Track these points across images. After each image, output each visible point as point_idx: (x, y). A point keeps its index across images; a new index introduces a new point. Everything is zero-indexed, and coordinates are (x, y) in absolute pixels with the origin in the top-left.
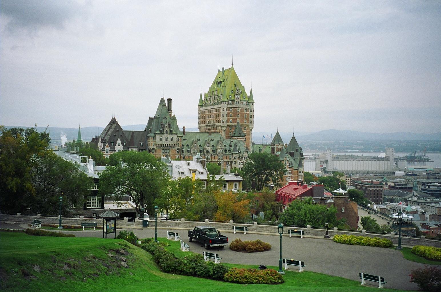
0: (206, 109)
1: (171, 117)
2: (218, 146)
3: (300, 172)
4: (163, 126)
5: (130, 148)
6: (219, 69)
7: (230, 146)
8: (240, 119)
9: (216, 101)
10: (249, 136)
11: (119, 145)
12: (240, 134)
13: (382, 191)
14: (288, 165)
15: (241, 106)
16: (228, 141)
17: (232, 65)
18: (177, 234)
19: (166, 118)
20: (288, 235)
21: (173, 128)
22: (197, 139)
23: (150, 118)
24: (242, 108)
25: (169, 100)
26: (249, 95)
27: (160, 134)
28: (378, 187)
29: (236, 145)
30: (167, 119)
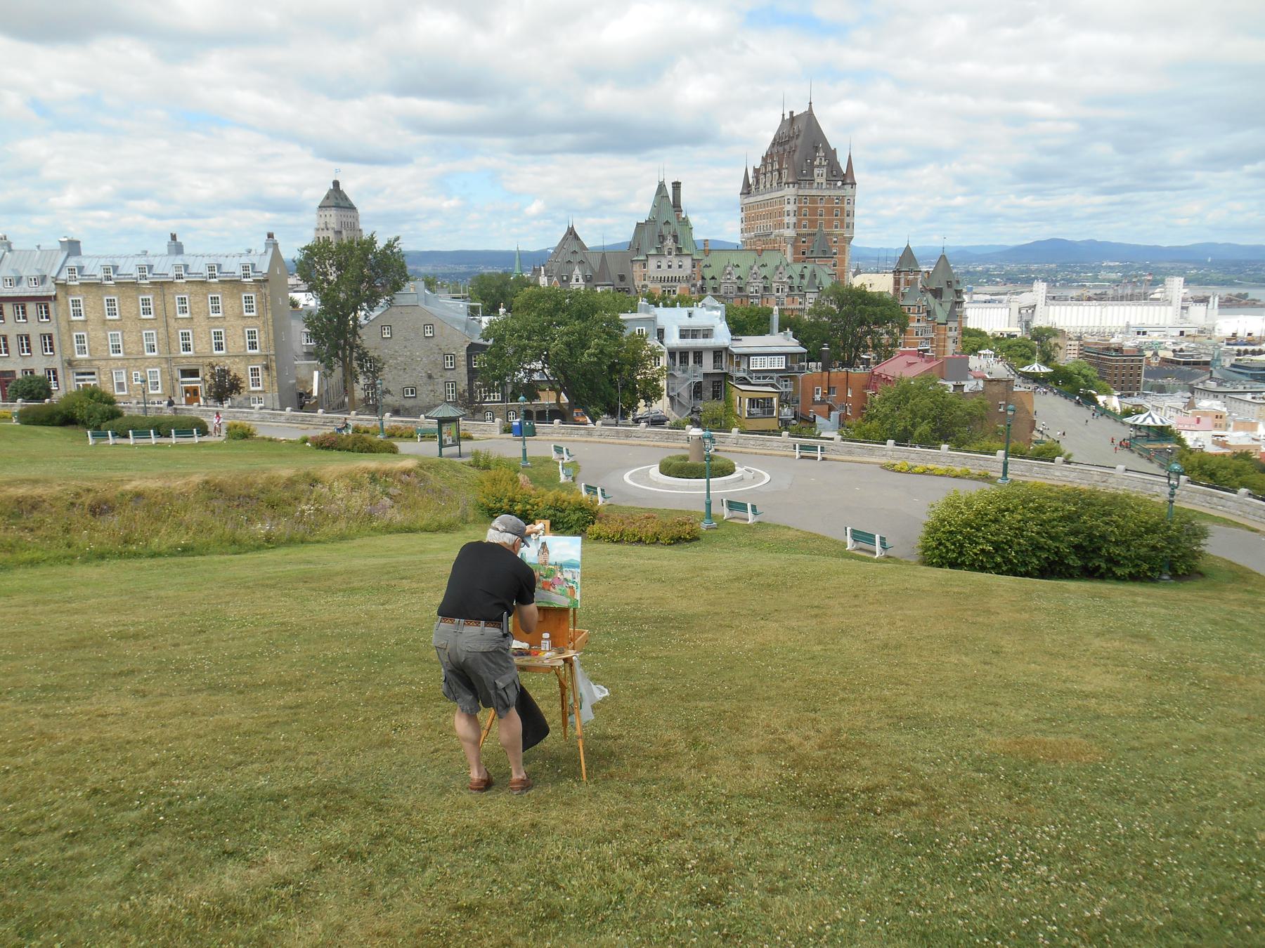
1: (681, 219)
2: (776, 278)
4: (662, 238)
5: (599, 285)
6: (783, 115)
7: (802, 277)
9: (775, 184)
11: (577, 280)
12: (824, 252)
13: (1140, 368)
14: (925, 314)
15: (827, 193)
16: (798, 268)
17: (810, 103)
18: (567, 450)
19: (667, 222)
20: (792, 454)
21: (684, 243)
23: (638, 224)
28: (1132, 361)
29: (814, 276)
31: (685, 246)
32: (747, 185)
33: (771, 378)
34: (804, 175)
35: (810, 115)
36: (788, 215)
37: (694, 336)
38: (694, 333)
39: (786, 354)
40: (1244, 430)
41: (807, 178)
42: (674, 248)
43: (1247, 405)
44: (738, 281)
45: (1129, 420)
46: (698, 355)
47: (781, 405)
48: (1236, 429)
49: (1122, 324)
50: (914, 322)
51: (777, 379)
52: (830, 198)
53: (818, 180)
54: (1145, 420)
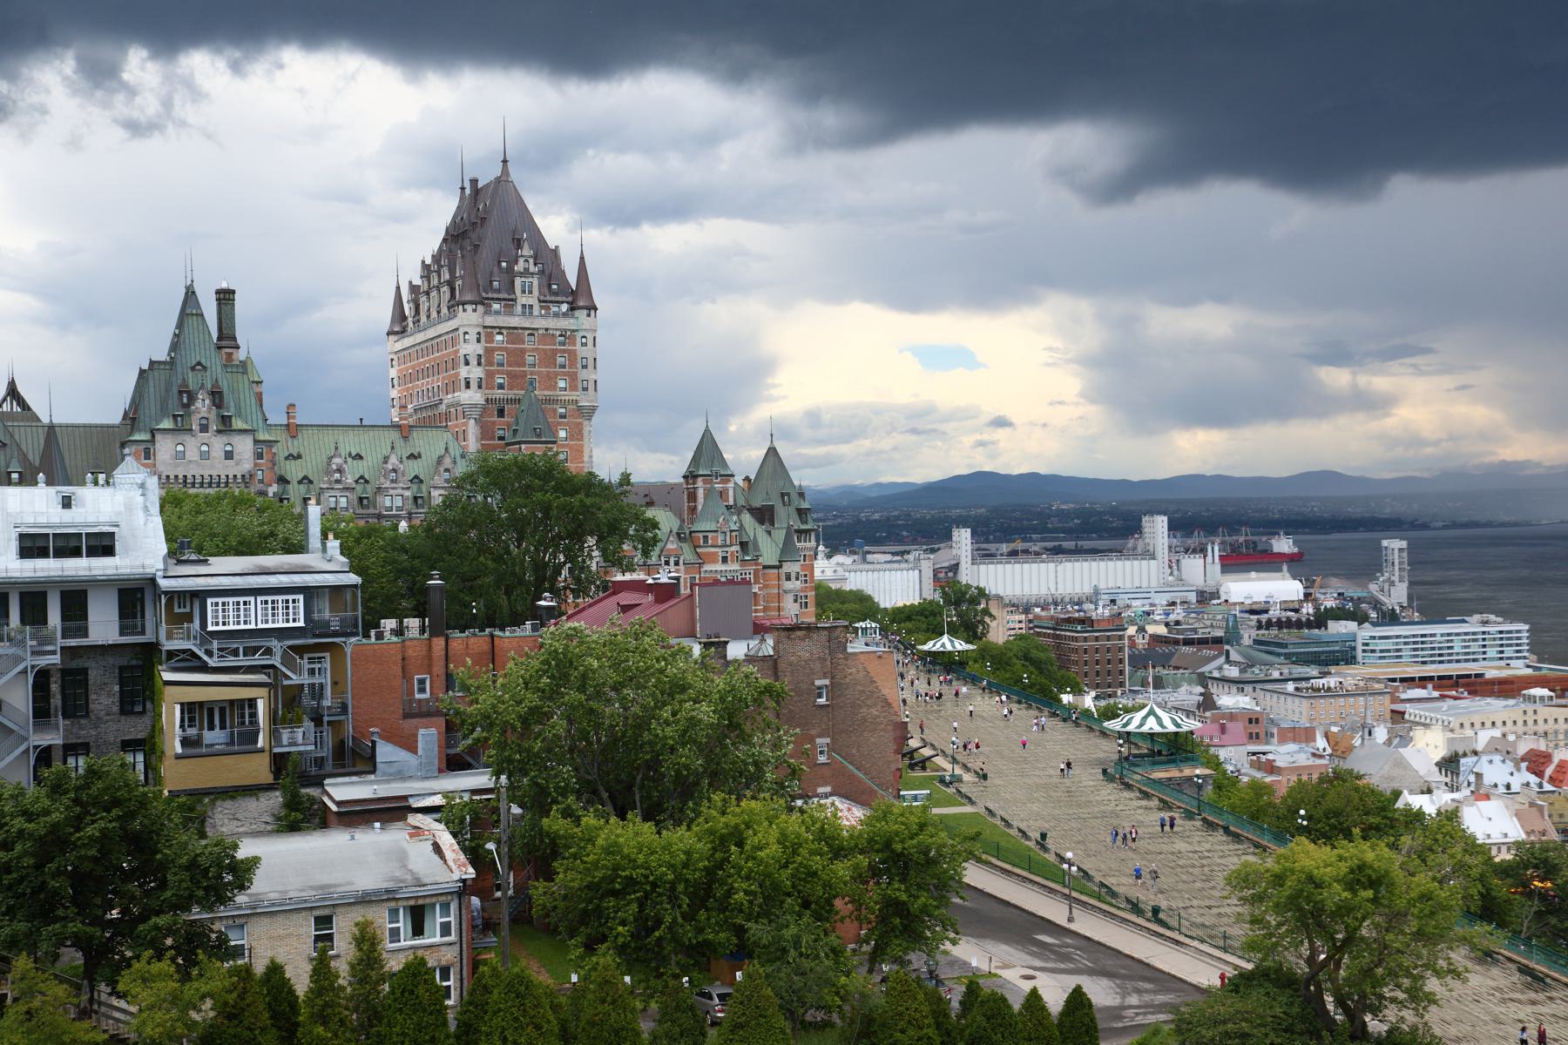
0: (414, 346)
3: (788, 578)
8: (539, 373)
9: (444, 310)
10: (582, 439)
13: (1121, 649)
14: (736, 548)
17: (505, 161)
19: (199, 367)
22: (350, 455)
24: (547, 330)
25: (222, 296)
26: (573, 281)
27: (174, 430)
28: (1108, 639)
30: (208, 373)
31: (239, 414)
32: (399, 315)
33: (269, 651)
34: (499, 291)
35: (503, 181)
36: (467, 363)
37: (61, 553)
38: (68, 545)
39: (308, 591)
40: (1294, 740)
41: (501, 296)
42: (213, 416)
43: (1289, 699)
44: (359, 488)
45: (1114, 725)
46: (75, 599)
47: (274, 719)
48: (1282, 741)
49: (1088, 590)
50: (715, 562)
51: (285, 656)
52: (548, 334)
53: (523, 300)
54: (1141, 725)
